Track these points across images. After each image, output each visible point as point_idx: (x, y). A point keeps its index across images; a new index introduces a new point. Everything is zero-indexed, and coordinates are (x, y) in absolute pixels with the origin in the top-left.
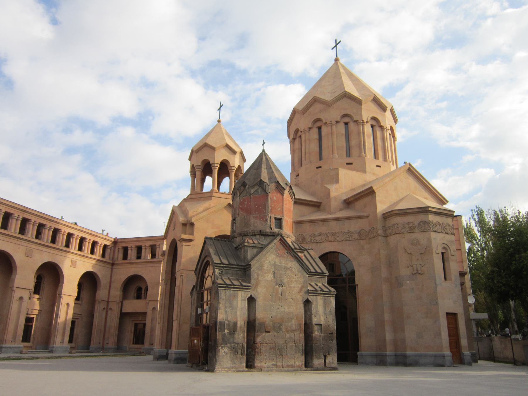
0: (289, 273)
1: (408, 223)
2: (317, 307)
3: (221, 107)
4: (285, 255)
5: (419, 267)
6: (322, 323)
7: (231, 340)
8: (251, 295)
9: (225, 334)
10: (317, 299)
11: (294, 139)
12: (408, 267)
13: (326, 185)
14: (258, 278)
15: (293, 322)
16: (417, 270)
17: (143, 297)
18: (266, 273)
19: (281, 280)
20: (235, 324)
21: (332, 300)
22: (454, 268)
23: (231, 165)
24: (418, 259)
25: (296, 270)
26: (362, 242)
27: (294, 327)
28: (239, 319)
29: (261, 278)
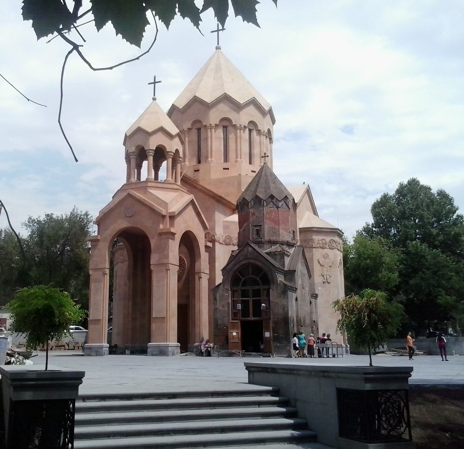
1: (322, 240)
5: (328, 276)
11: (190, 129)
12: (320, 276)
16: (327, 279)
24: (327, 271)
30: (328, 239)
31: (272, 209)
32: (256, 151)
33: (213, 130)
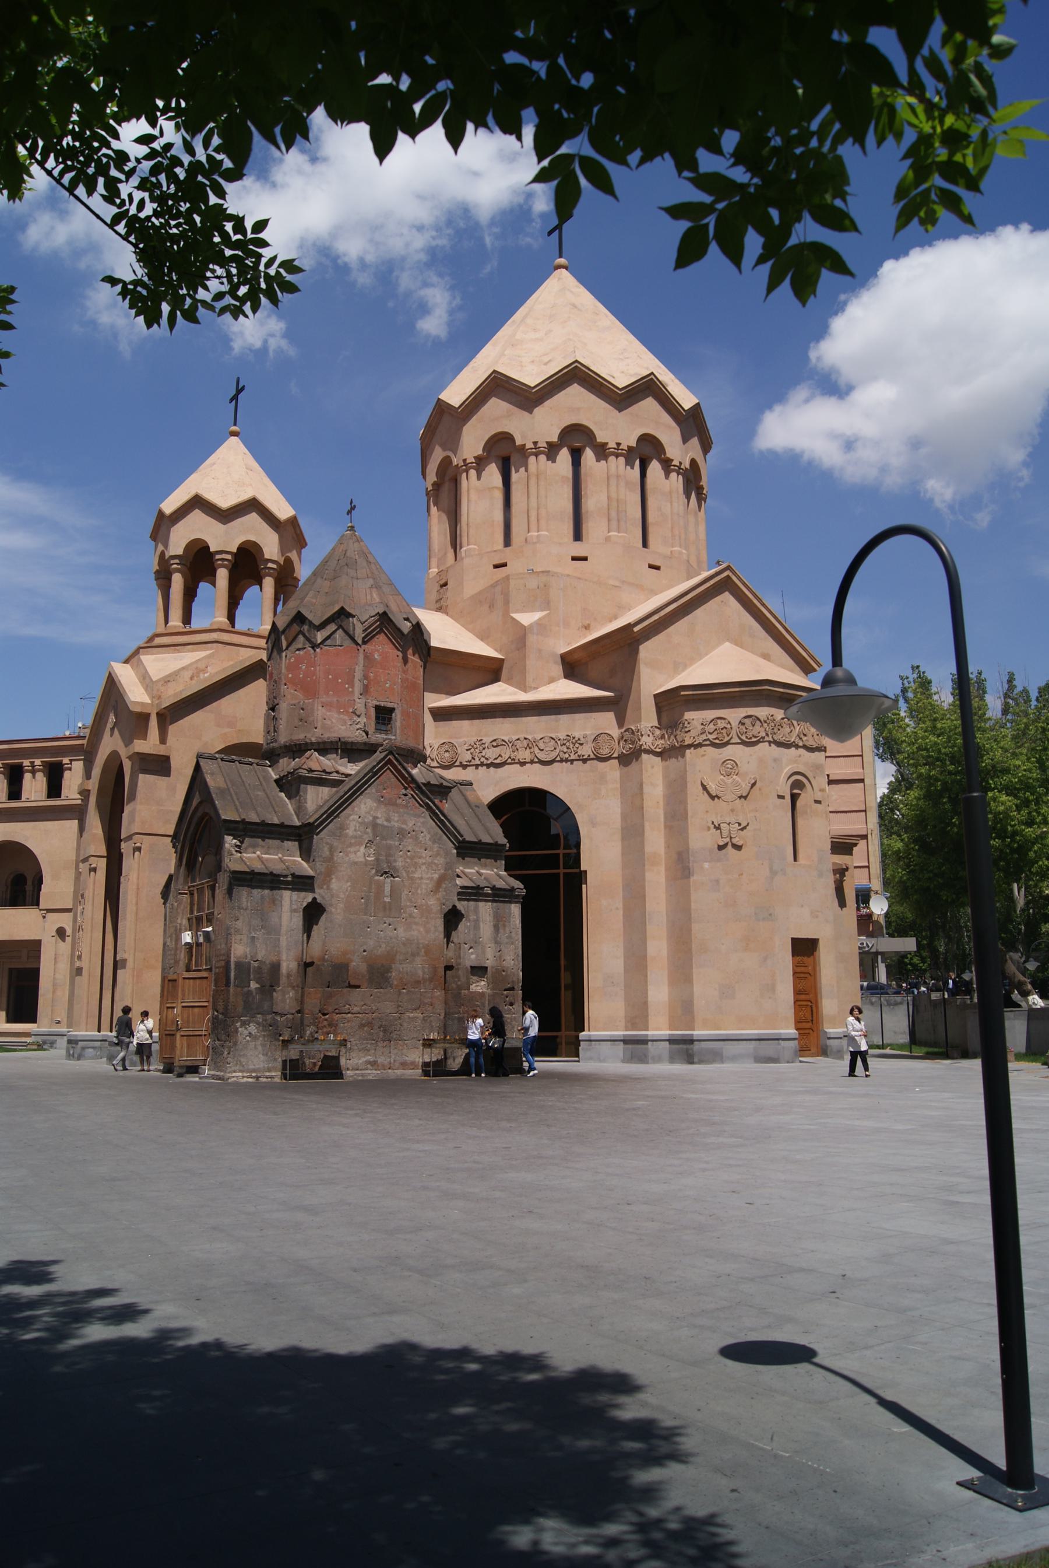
0: (409, 843)
2: (477, 927)
3: (239, 391)
4: (399, 801)
6: (488, 963)
7: (266, 1006)
8: (314, 899)
9: (250, 992)
10: (477, 907)
12: (709, 829)
13: (514, 615)
14: (330, 859)
15: (419, 962)
17: (28, 899)
18: (351, 845)
19: (388, 862)
20: (276, 967)
21: (515, 910)
22: (818, 831)
23: (267, 556)
24: (732, 810)
25: (428, 836)
26: (601, 765)
27: (420, 973)
28: (284, 957)
29: (339, 857)
30: (734, 715)
31: (301, 653)
32: (592, 502)
33: (473, 473)
